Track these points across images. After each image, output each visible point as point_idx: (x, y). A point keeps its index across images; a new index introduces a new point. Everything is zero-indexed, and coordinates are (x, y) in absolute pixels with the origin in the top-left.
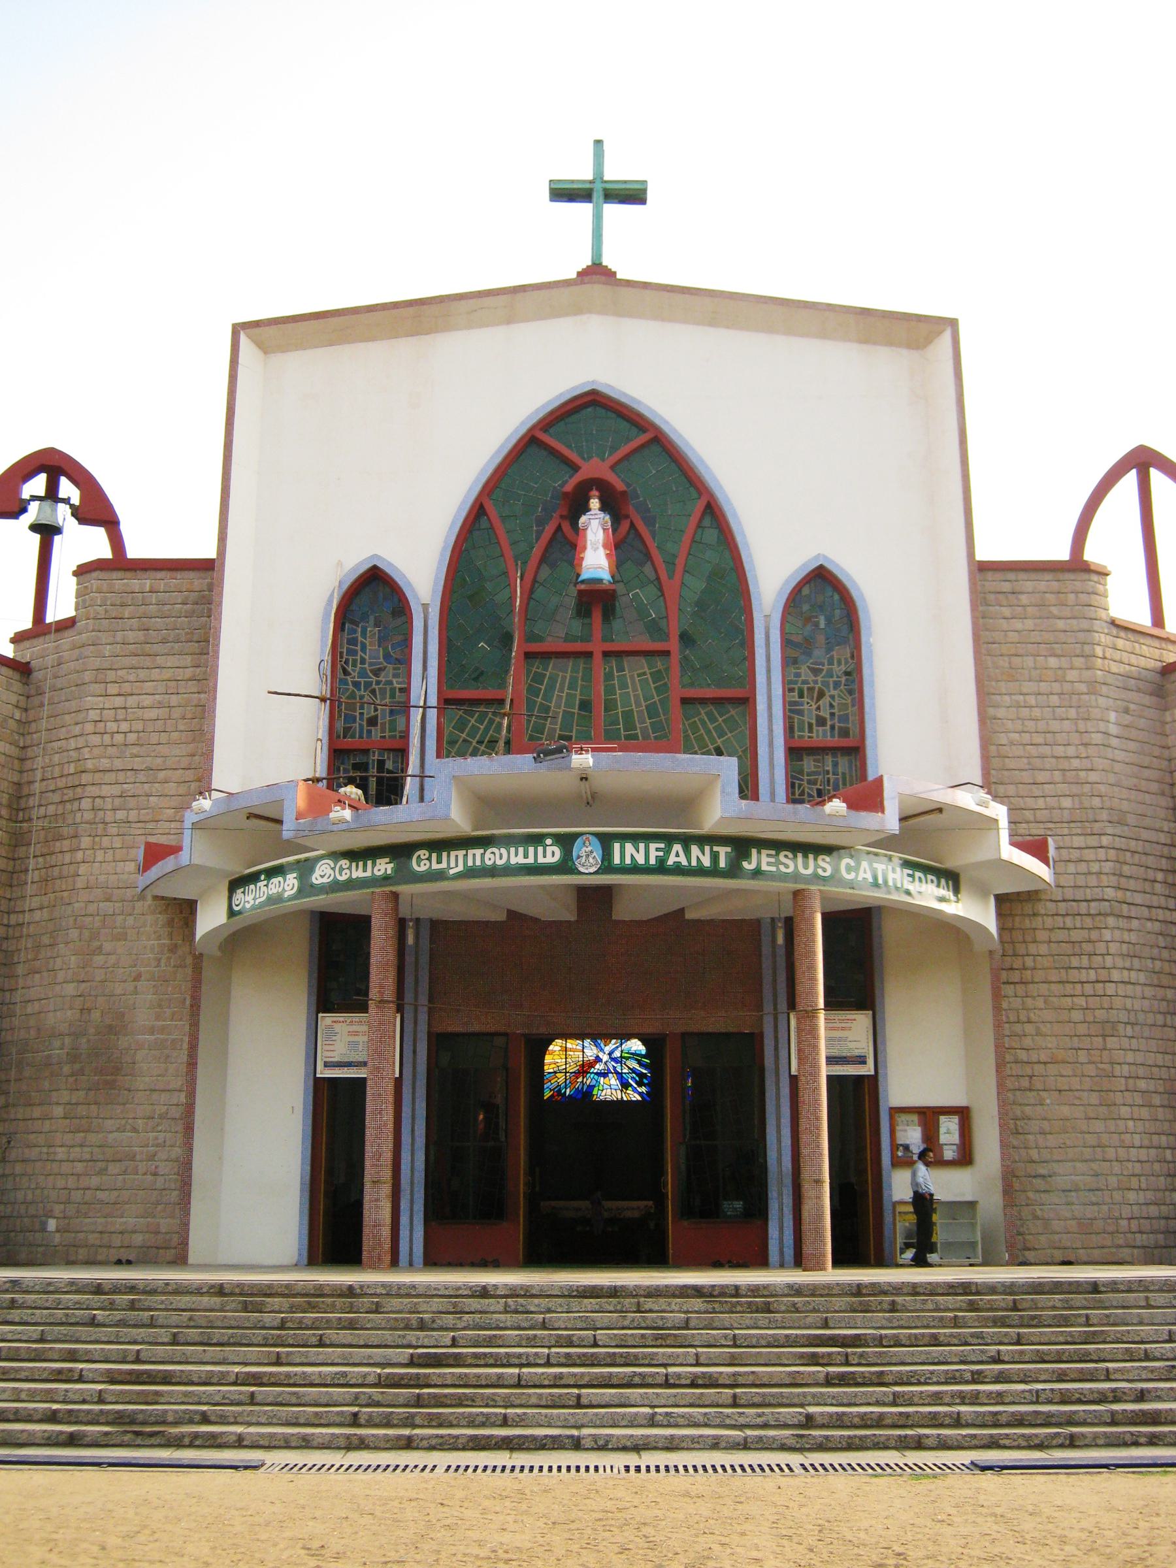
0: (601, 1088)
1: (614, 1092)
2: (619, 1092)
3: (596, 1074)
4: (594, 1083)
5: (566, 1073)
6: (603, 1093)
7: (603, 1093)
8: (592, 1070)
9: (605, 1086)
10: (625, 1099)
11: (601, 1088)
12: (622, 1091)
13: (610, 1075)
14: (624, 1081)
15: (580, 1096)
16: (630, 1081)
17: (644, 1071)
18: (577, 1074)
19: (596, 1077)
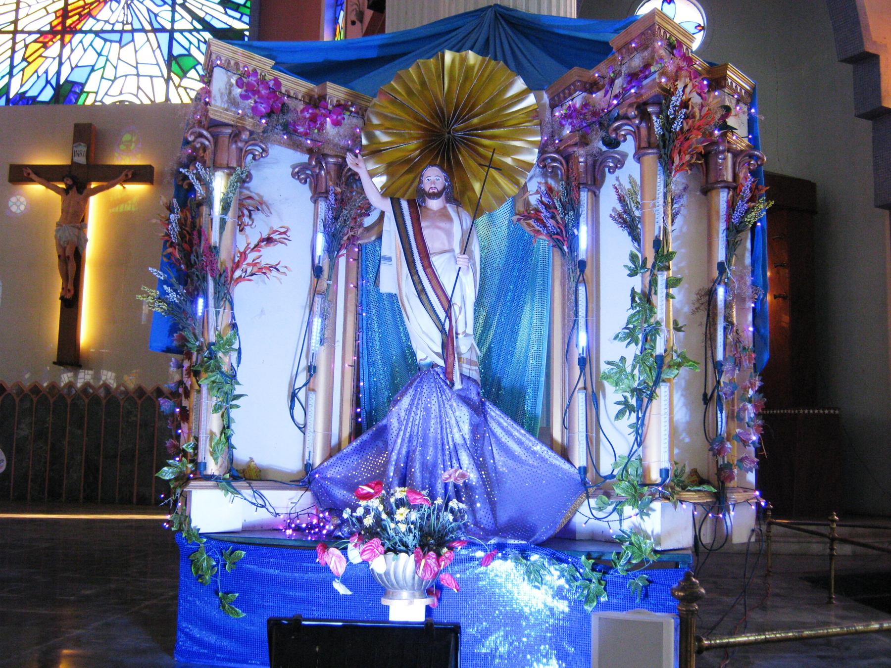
0: (110, 73)
1: (145, 83)
2: (160, 84)
3: (97, 34)
4: (90, 58)
5: (15, 32)
6: (115, 90)
7: (115, 90)
8: (89, 24)
9: (123, 69)
10: (175, 100)
11: (110, 73)
12: (168, 80)
13: (140, 37)
14: (177, 50)
15: (47, 95)
16: (194, 52)
17: (238, 25)
18: (46, 37)
19: (98, 43)
